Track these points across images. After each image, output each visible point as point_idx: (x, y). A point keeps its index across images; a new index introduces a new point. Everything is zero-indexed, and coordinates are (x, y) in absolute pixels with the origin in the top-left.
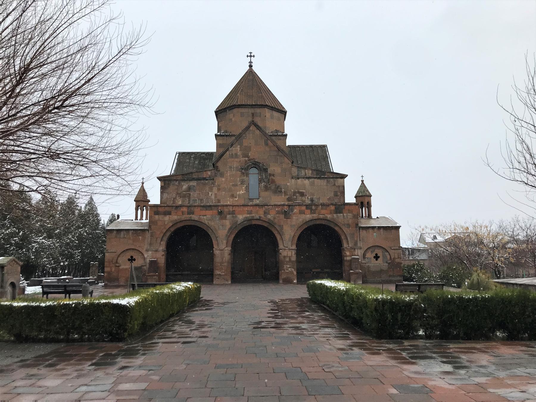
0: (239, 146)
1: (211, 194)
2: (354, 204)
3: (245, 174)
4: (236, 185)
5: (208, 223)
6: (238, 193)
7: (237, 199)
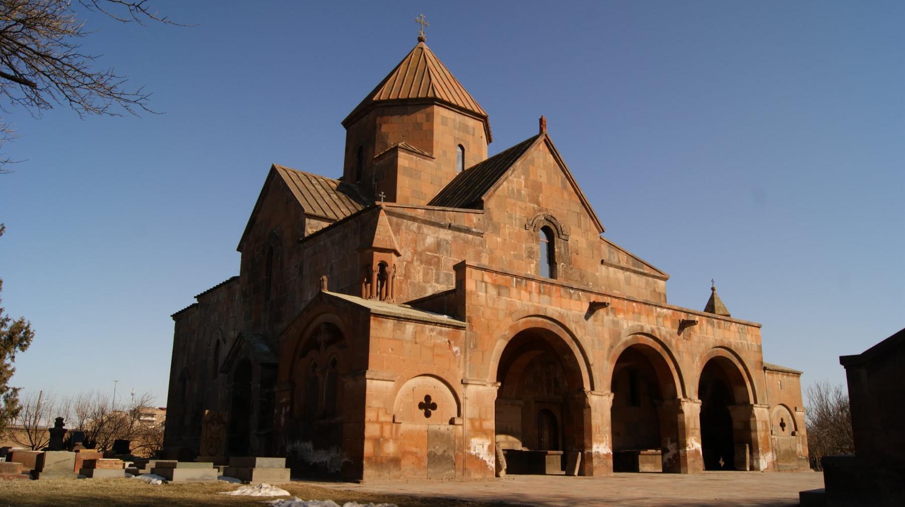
0: (523, 177)
5: (576, 330)
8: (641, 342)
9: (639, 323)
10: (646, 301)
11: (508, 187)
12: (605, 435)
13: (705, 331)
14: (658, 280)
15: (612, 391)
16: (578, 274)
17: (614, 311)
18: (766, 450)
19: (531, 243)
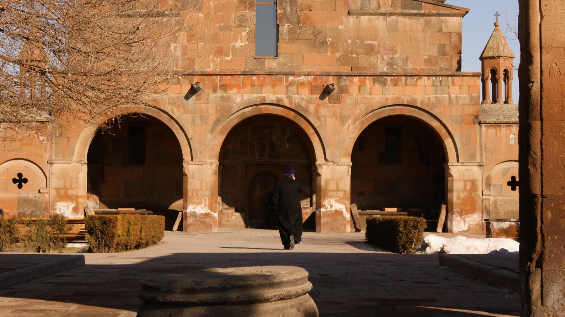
1: (176, 47)
2: (475, 75)
3: (247, 4)
4: (227, 28)
5: (172, 110)
6: (232, 45)
7: (229, 59)
8: (264, 112)
9: (260, 95)
10: (270, 72)
12: (204, 198)
13: (368, 91)
15: (219, 161)
16: (310, 32)
17: (223, 87)
18: (465, 212)
19: (244, 10)
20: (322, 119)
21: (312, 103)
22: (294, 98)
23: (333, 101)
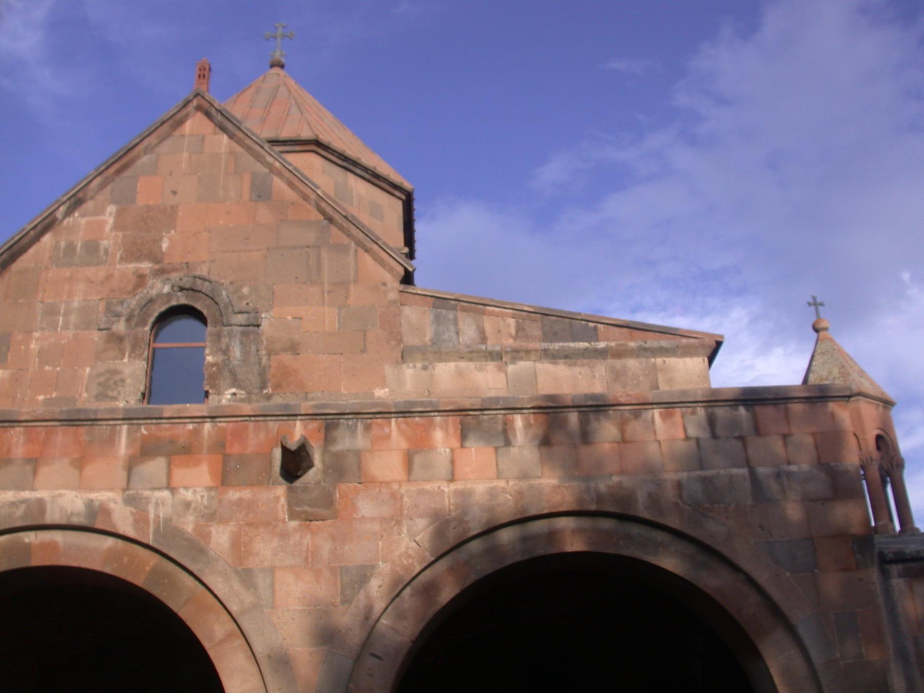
0: (111, 209)
8: (37, 561)
9: (26, 494)
11: (57, 243)
14: (671, 361)
19: (115, 358)
20: (262, 581)
21: (223, 521)
22: (154, 501)
23: (306, 508)
